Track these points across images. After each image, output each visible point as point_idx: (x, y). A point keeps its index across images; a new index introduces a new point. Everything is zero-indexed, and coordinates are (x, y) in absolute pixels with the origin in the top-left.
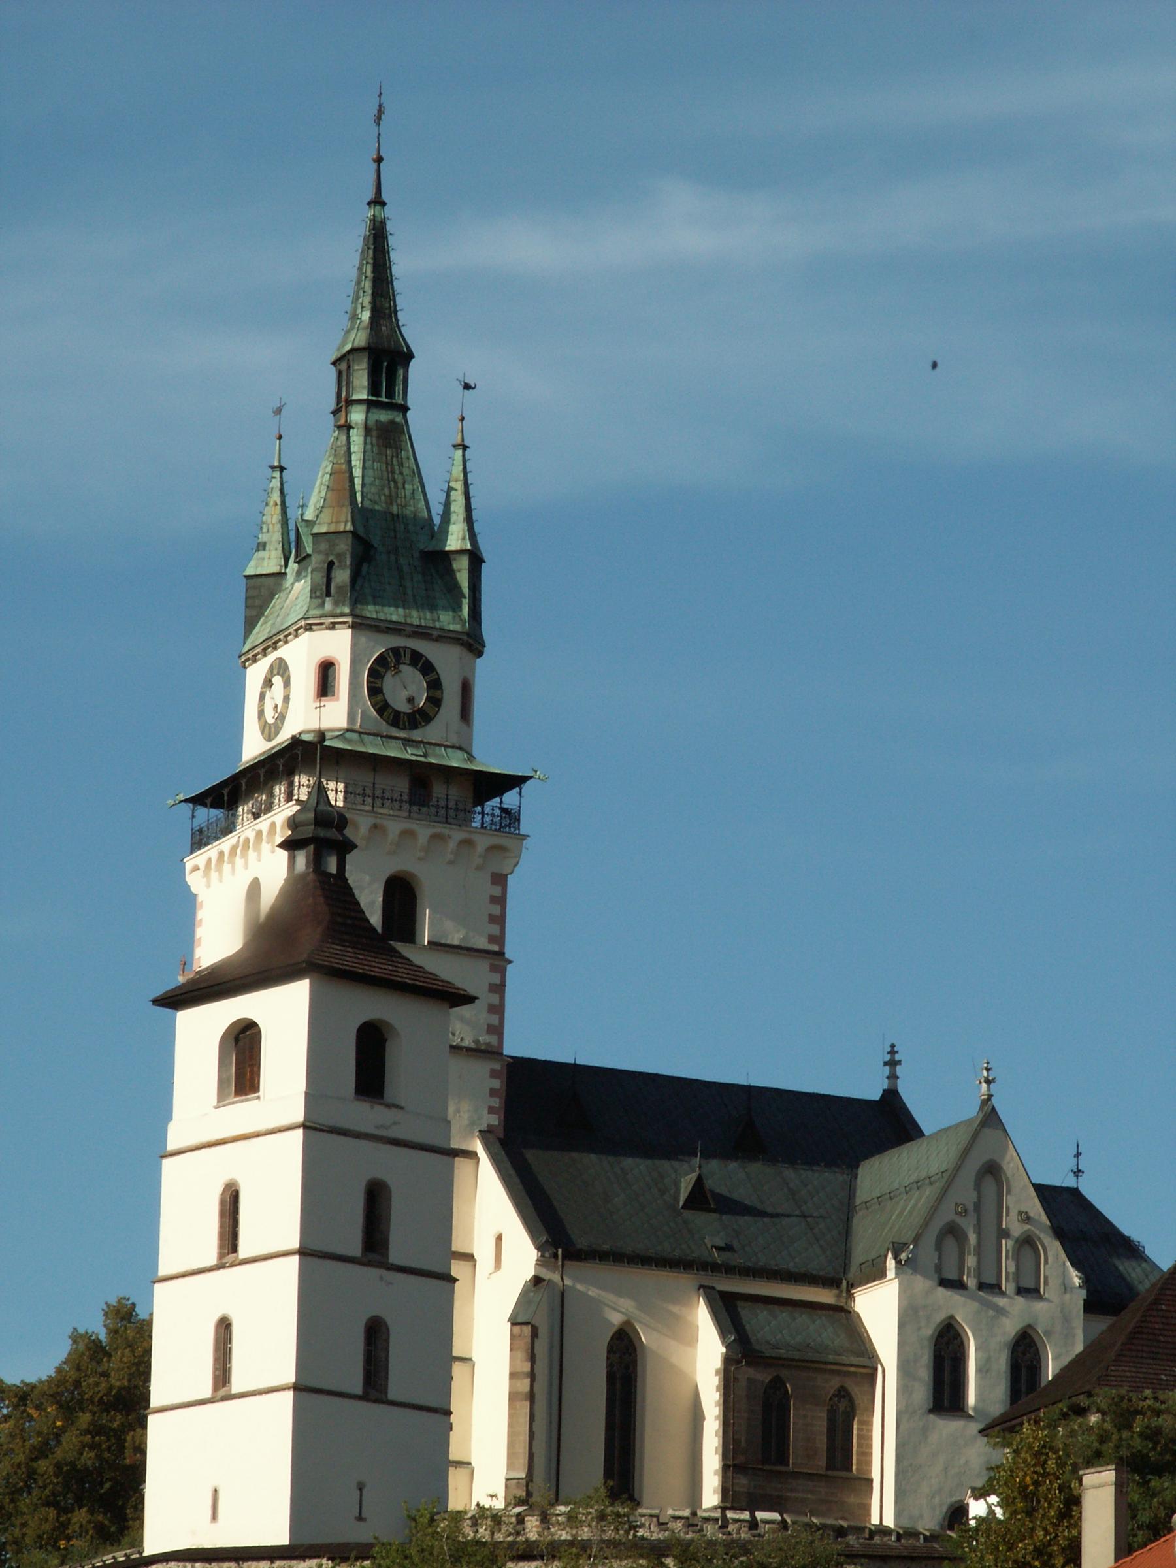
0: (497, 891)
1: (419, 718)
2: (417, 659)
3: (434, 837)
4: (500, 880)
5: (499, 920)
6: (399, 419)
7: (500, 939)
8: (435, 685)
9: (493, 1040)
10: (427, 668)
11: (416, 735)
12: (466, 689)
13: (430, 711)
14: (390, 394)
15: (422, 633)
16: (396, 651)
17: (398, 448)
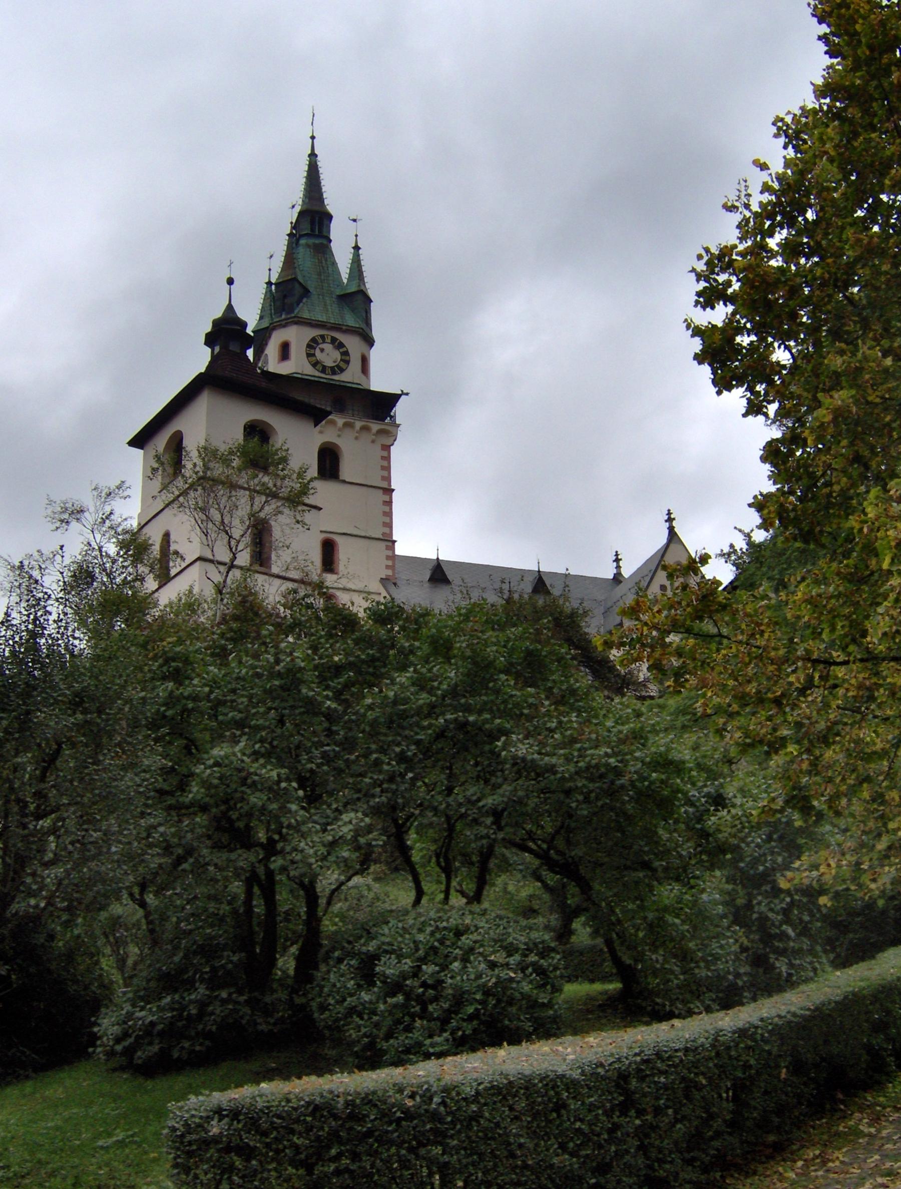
0: (385, 454)
1: (338, 369)
2: (334, 340)
3: (346, 425)
4: (387, 448)
5: (388, 469)
6: (325, 242)
7: (388, 479)
8: (346, 353)
9: (387, 530)
10: (341, 345)
11: (336, 377)
12: (365, 361)
13: (342, 365)
14: (320, 231)
15: (337, 328)
16: (322, 337)
17: (324, 253)
